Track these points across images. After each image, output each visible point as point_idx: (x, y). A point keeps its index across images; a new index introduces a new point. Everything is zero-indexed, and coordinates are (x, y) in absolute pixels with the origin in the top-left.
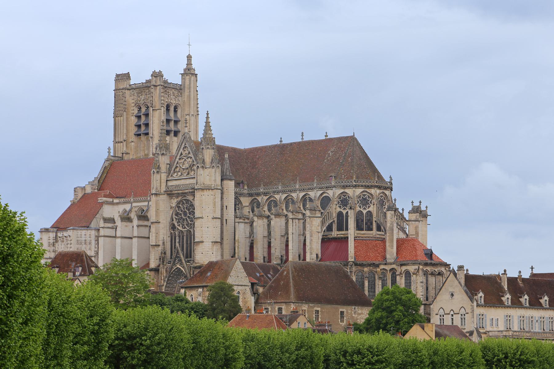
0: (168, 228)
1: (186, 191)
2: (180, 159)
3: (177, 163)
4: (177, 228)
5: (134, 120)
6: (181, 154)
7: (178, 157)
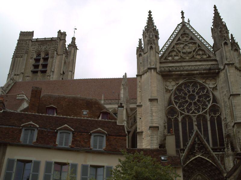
0: (164, 113)
1: (196, 72)
2: (176, 44)
3: (174, 47)
4: (180, 112)
5: (32, 62)
6: (179, 39)
7: (175, 42)
